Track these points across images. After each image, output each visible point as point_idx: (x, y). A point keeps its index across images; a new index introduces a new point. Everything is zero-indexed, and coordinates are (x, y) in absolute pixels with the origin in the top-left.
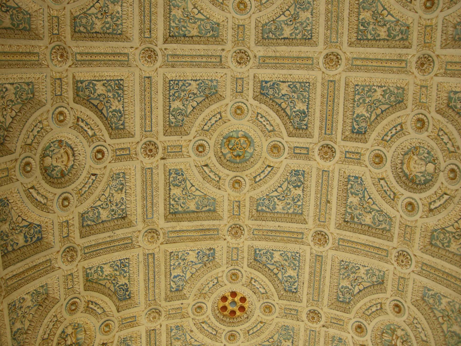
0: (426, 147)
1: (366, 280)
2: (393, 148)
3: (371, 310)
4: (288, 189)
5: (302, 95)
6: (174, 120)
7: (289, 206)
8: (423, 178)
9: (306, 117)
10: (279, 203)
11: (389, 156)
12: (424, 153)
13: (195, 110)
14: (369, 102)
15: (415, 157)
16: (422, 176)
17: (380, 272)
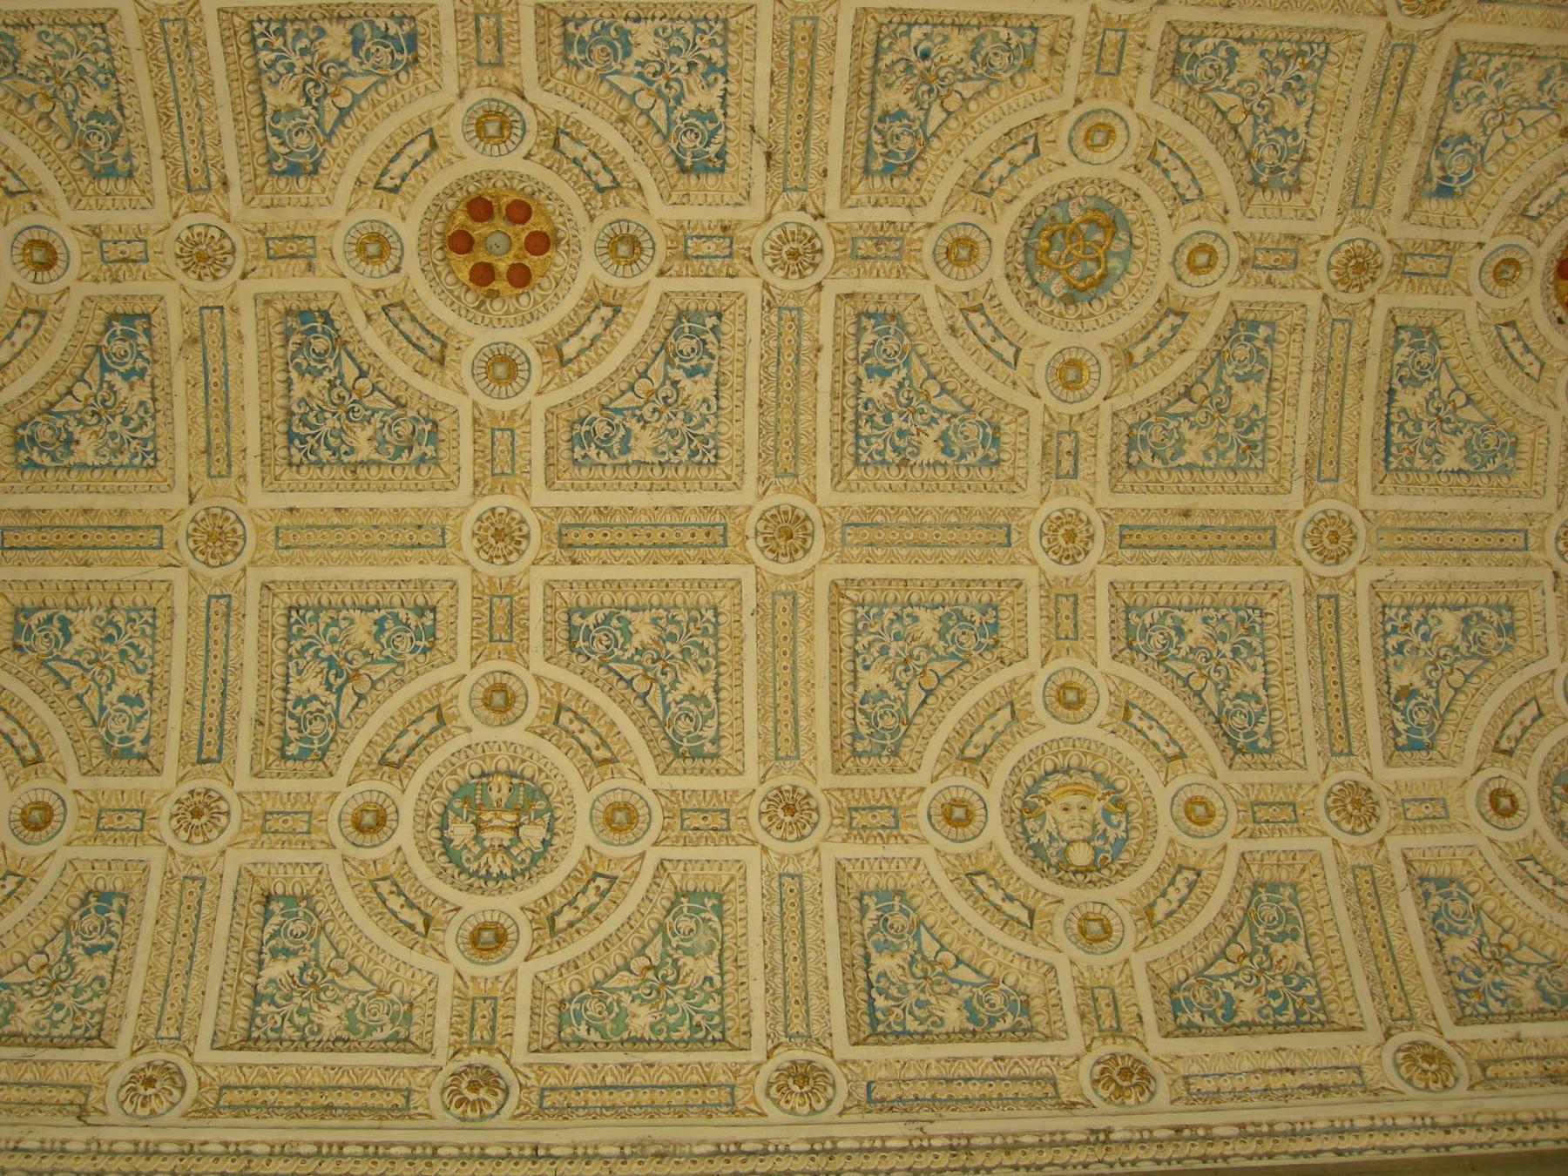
0: (1133, 834)
1: (670, 698)
2: (1110, 740)
3: (582, 731)
4: (936, 415)
5: (1231, 447)
6: (1200, 48)
7: (878, 419)
8: (1045, 839)
9: (1165, 462)
10: (887, 388)
11: (1087, 730)
12: (1114, 827)
13: (1219, 116)
14: (1219, 651)
15: (1096, 806)
16: (1050, 835)
17: (713, 742)
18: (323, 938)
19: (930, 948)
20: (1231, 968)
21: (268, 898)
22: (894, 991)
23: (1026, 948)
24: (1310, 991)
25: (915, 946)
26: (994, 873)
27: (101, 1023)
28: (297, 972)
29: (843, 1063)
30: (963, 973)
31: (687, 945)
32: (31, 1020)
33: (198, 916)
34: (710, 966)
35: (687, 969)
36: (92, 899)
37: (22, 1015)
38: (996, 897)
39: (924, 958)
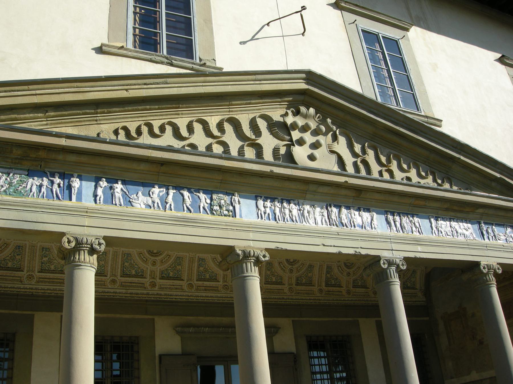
18: (51, 255)
19: (132, 262)
20: (171, 269)
21: (43, 248)
22: (127, 268)
23: (145, 265)
24: (180, 273)
25: (131, 262)
26: (143, 254)
27: (20, 266)
28: (47, 259)
29: (119, 280)
30: (136, 266)
31: (101, 259)
32: (10, 265)
33: (34, 252)
34: (103, 263)
35: (100, 263)
36: (17, 247)
37: (9, 265)
38: (143, 257)
39: (131, 264)
